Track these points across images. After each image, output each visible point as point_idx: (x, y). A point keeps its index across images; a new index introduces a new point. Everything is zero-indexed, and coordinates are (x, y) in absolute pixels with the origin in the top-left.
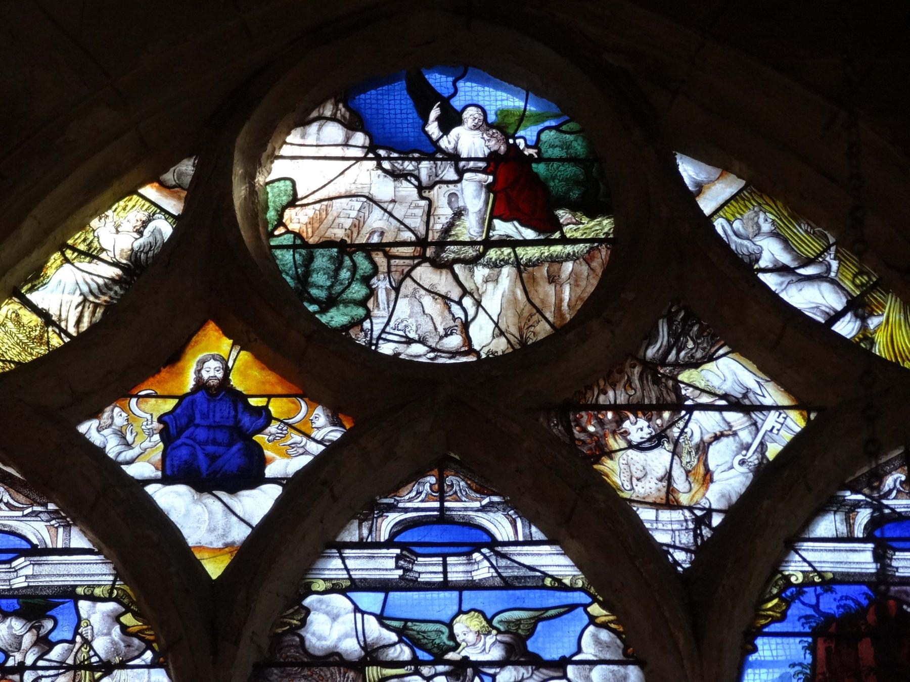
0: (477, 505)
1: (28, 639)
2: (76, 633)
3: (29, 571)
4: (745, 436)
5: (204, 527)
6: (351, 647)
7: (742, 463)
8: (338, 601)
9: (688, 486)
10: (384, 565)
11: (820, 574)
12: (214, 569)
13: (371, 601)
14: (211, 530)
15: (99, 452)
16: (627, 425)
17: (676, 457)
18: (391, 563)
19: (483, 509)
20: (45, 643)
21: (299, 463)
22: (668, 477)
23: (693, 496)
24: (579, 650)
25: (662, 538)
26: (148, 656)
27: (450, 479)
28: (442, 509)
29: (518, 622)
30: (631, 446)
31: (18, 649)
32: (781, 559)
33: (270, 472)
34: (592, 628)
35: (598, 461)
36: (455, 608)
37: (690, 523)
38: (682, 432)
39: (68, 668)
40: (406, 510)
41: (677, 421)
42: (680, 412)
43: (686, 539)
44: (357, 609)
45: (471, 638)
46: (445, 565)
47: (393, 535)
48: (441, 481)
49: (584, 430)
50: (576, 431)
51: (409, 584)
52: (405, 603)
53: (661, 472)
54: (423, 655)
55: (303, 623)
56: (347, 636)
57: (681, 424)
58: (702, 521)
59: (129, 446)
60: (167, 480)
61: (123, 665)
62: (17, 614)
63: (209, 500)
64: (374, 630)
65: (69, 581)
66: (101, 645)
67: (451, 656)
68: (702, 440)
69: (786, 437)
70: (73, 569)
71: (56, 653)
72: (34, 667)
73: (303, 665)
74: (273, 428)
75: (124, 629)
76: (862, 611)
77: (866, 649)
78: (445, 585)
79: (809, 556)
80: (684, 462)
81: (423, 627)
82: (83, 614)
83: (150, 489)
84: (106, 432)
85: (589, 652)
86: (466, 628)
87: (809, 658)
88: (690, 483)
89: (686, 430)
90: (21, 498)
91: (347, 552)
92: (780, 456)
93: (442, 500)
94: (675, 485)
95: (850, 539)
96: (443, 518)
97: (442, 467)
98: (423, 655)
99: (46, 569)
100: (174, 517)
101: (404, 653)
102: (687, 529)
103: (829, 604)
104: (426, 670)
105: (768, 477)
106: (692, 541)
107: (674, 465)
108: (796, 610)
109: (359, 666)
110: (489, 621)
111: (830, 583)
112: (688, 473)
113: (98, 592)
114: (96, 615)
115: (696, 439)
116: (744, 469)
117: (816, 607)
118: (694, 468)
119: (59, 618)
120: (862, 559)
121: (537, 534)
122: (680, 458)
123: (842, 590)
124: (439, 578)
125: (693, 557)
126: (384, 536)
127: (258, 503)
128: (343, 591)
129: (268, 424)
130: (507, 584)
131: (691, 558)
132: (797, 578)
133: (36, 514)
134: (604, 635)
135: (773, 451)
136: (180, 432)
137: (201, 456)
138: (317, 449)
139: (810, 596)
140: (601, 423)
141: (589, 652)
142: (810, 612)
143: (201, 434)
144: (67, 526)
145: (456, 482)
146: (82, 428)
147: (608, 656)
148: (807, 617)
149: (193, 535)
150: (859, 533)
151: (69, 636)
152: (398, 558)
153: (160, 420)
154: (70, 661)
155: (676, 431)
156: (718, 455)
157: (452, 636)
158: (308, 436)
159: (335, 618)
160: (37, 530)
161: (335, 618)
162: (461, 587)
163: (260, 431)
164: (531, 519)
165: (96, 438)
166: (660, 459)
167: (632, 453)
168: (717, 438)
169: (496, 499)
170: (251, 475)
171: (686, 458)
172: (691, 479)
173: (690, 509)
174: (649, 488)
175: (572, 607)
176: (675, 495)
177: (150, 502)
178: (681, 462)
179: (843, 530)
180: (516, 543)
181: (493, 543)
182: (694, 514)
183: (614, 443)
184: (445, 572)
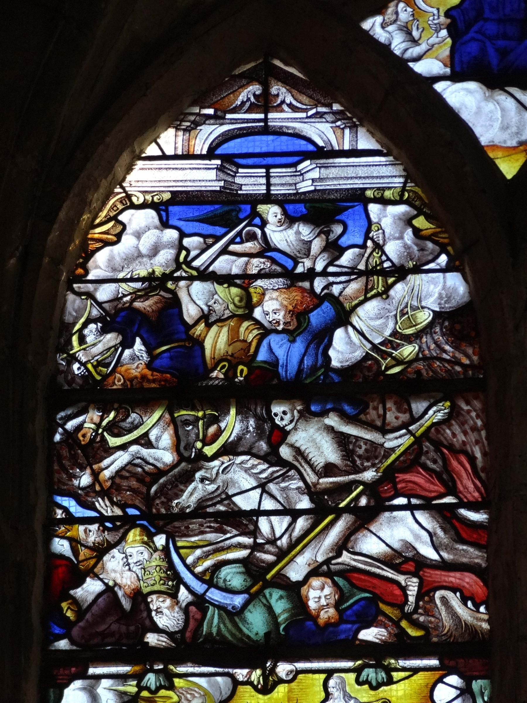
1: (317, 245)
2: (367, 237)
3: (315, 174)
5: (497, 125)
12: (509, 168)
14: (504, 128)
15: (385, 49)
20: (334, 249)
26: (443, 259)
31: (307, 254)
39: (360, 274)
59: (415, 42)
60: (455, 77)
61: (417, 270)
62: (305, 219)
63: (502, 97)
65: (358, 184)
66: (393, 249)
70: (361, 171)
71: (347, 258)
72: (324, 273)
75: (417, 232)
82: (374, 217)
83: (439, 87)
84: (390, 28)
90: (304, 99)
99: (333, 172)
100: (465, 116)
113: (388, 194)
114: (387, 218)
119: (350, 223)
133: (320, 115)
136: (469, 26)
137: (491, 51)
143: (491, 28)
144: (353, 127)
146: (366, 25)
149: (486, 134)
151: (359, 241)
153: (447, 14)
154: (362, 267)
160: (322, 132)
165: (380, 35)
177: (439, 98)
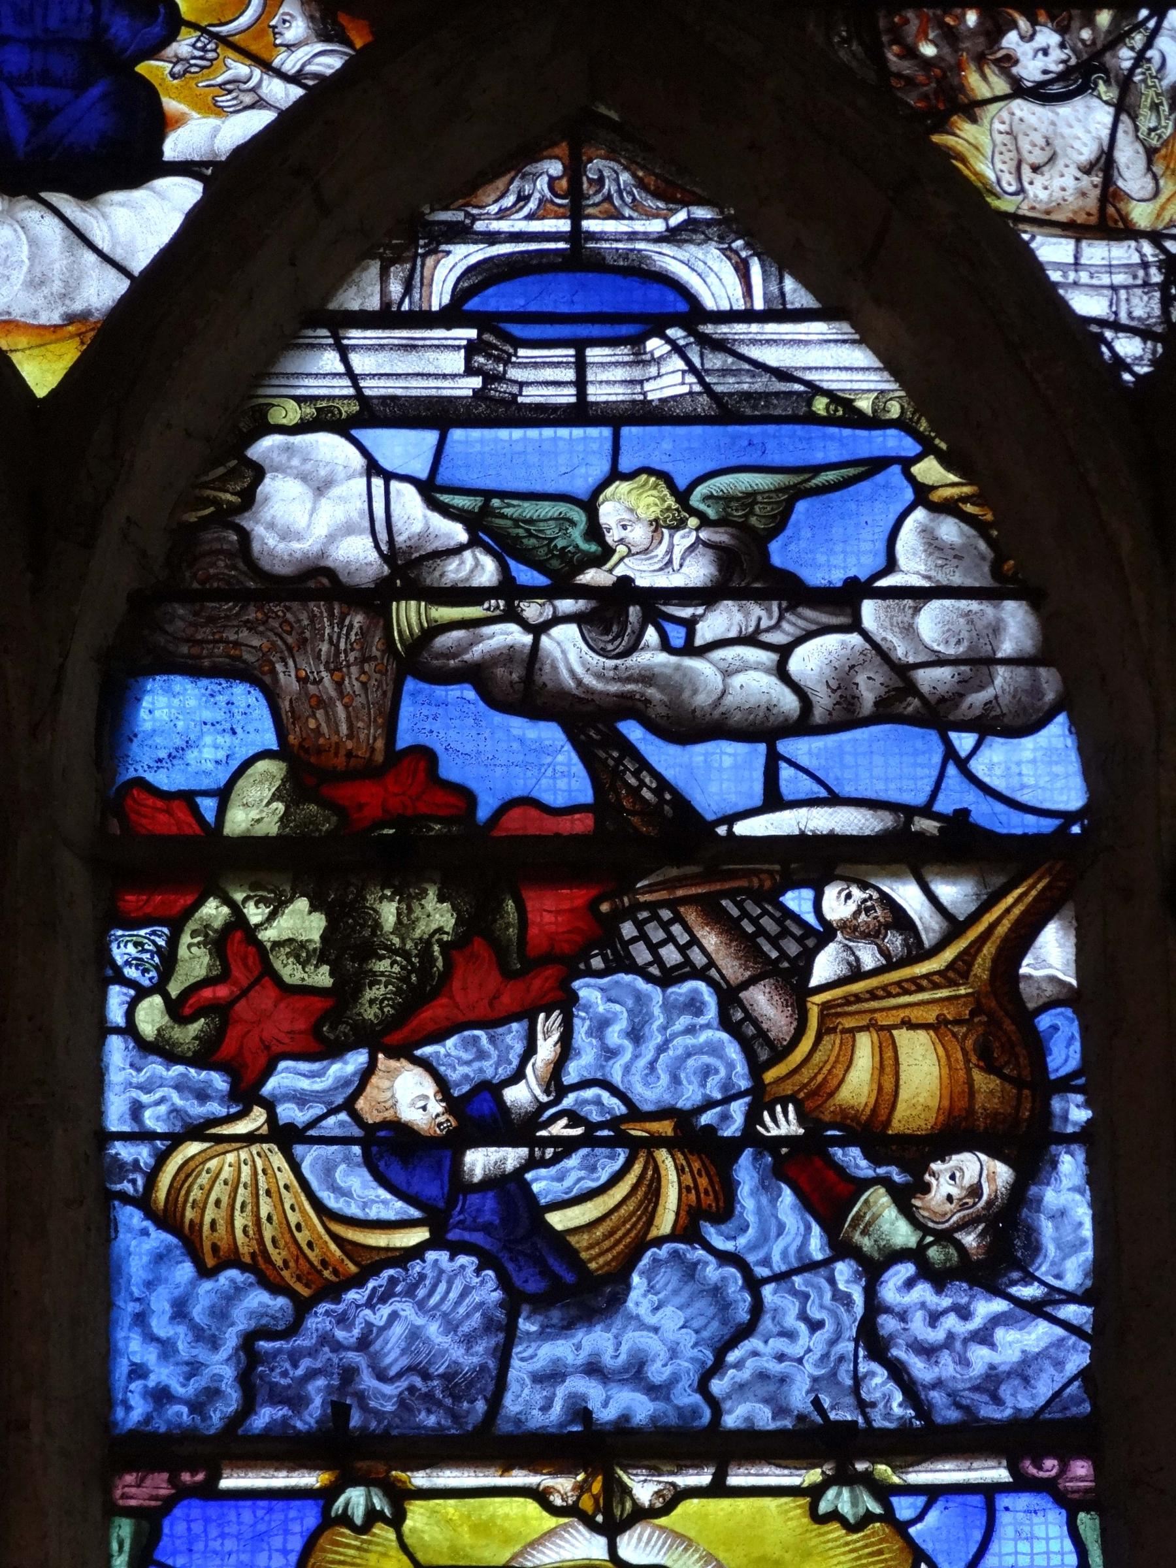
0: (657, 226)
5: (19, 276)
6: (358, 554)
8: (329, 447)
9: (1150, 186)
10: (440, 365)
12: (42, 373)
13: (406, 448)
14: (36, 283)
16: (1011, 40)
17: (1124, 117)
18: (455, 362)
19: (672, 236)
21: (247, 125)
22: (1104, 164)
23: (1163, 208)
24: (891, 566)
25: (1087, 305)
27: (596, 166)
28: (576, 236)
29: (749, 498)
30: (1019, 90)
33: (174, 147)
34: (920, 514)
35: (943, 126)
36: (601, 468)
37: (1153, 271)
38: (1140, 58)
40: (492, 238)
41: (1128, 34)
42: (1136, 12)
43: (1144, 307)
44: (373, 468)
45: (639, 534)
46: (581, 365)
47: (460, 295)
48: (574, 171)
49: (911, 53)
50: (892, 55)
51: (497, 409)
52: (482, 453)
53: (1087, 152)
54: (526, 575)
55: (248, 499)
56: (348, 529)
57: (1138, 39)
64: (412, 513)
67: (592, 577)
73: (245, 597)
74: (183, 46)
78: (581, 413)
80: (1143, 129)
81: (529, 509)
85: (913, 567)
86: (626, 511)
88: (1155, 178)
89: (1149, 54)
91: (355, 336)
93: (576, 214)
94: (1120, 183)
96: (579, 256)
97: (577, 138)
98: (526, 575)
101: (482, 569)
102: (1146, 284)
104: (532, 611)
106: (1157, 312)
107: (1120, 135)
109: (374, 599)
110: (682, 497)
112: (1151, 153)
118: (1165, 143)
121: (797, 295)
122: (1134, 118)
124: (567, 396)
125: (1160, 350)
126: (440, 295)
127: (146, 220)
128: (342, 427)
129: (171, 36)
130: (725, 411)
131: (1154, 352)
134: (950, 530)
138: (283, 94)
140: (951, 36)
141: (913, 567)
145: (611, 174)
147: (957, 580)
152: (471, 349)
155: (1125, 57)
157: (595, 531)
158: (267, 66)
159: (321, 488)
161: (321, 488)
162: (616, 418)
163: (154, 51)
164: (781, 261)
166: (1086, 122)
167: (1021, 108)
169: (701, 213)
170: (133, 157)
171: (1147, 120)
172: (1158, 169)
173: (1156, 237)
174: (1060, 187)
175: (876, 465)
176: (1121, 205)
178: (1137, 129)
180: (748, 316)
181: (693, 315)
182: (1164, 250)
183: (979, 84)
184: (581, 383)
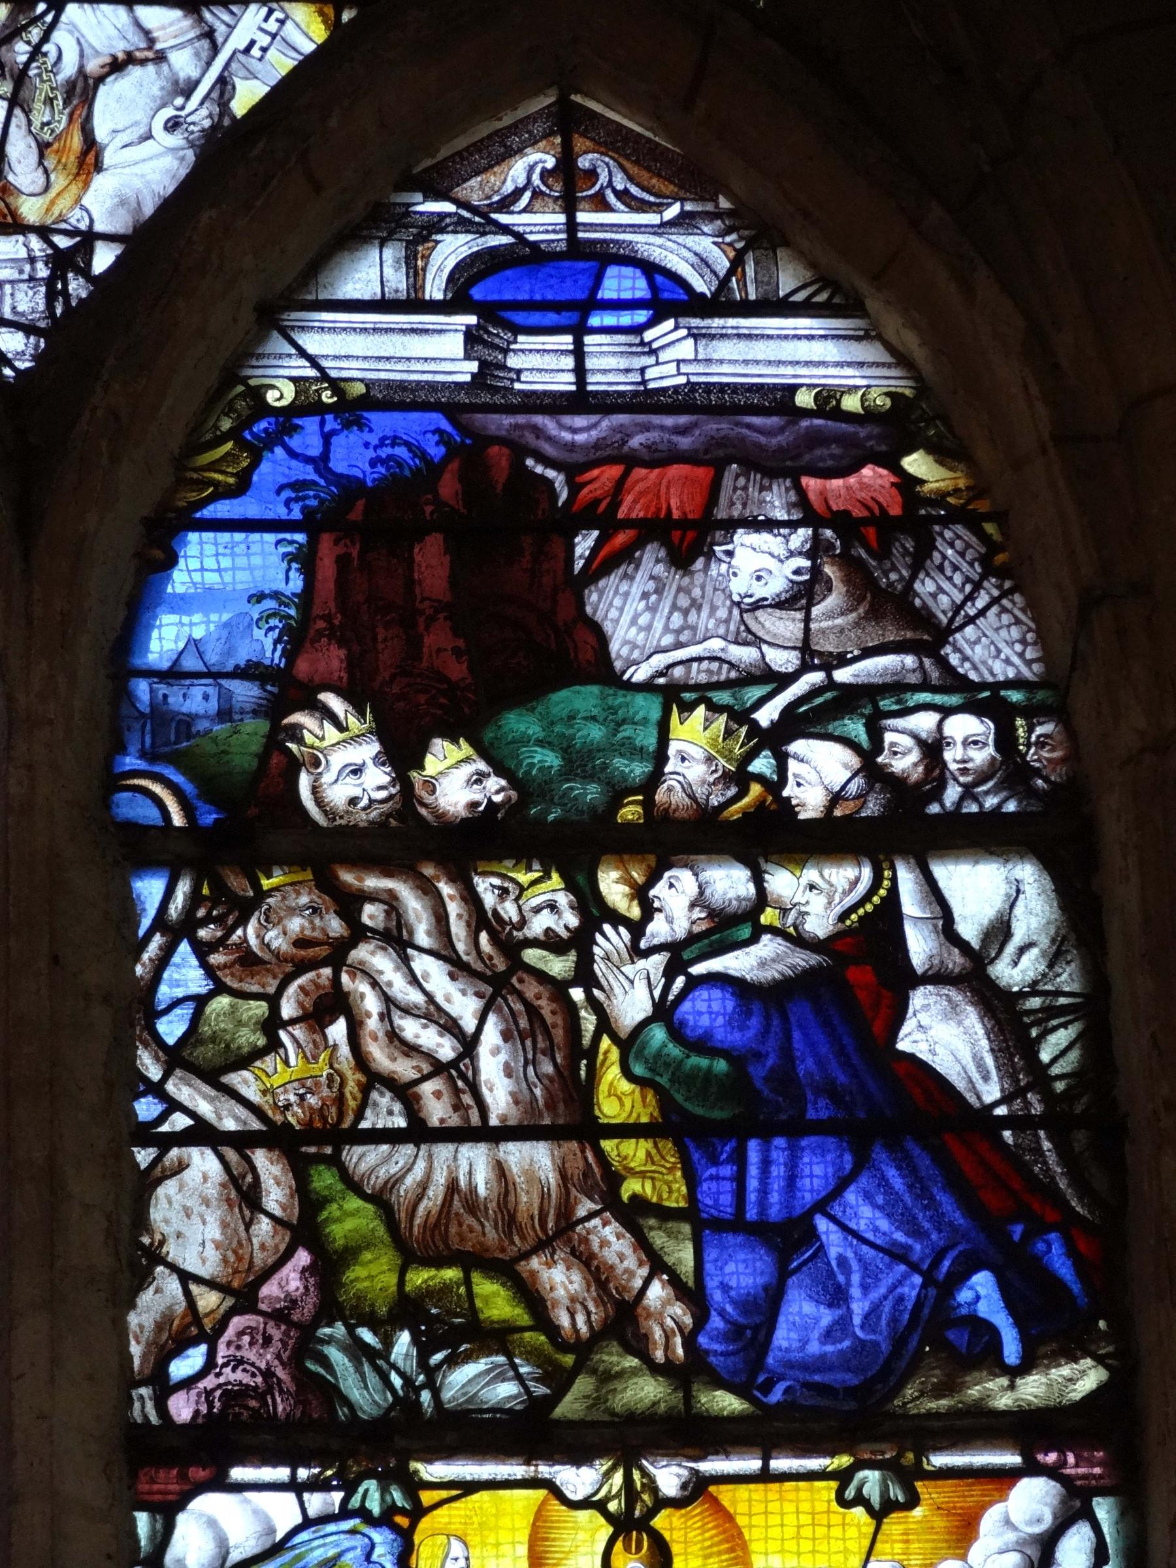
4: (184, 63)
7: (173, 125)
9: (41, 180)
11: (336, 385)
17: (17, 112)
23: (53, 203)
32: (248, 351)
37: (40, 265)
38: (36, 52)
41: (25, 28)
42: (33, 6)
57: (35, 34)
58: (64, 263)
68: (81, 70)
69: (281, 64)
76: (431, 470)
77: (431, 562)
79: (312, 343)
80: (36, 123)
87: (296, 583)
88: (46, 171)
89: (45, 48)
92: (257, 110)
94: (11, 178)
95: (415, 304)
102: (31, 279)
103: (352, 455)
105: (231, 157)
106: (42, 307)
107: (13, 129)
108: (275, 467)
111: (353, 406)
112: (43, 148)
115: (69, 68)
116: (176, 140)
117: (321, 462)
118: (58, 138)
120: (439, 352)
122: (27, 113)
123: (384, 423)
125: (42, 345)
131: (37, 346)
132: (281, 395)
135: (247, 96)
139: (308, 438)
142: (308, 473)
148: (298, 486)
150: (435, 290)
156: (119, 107)
168: (117, 66)
171: (41, 114)
172: (50, 163)
173: (44, 232)
176: (10, 200)
178: (30, 123)
179: (398, 282)
182: (52, 245)
